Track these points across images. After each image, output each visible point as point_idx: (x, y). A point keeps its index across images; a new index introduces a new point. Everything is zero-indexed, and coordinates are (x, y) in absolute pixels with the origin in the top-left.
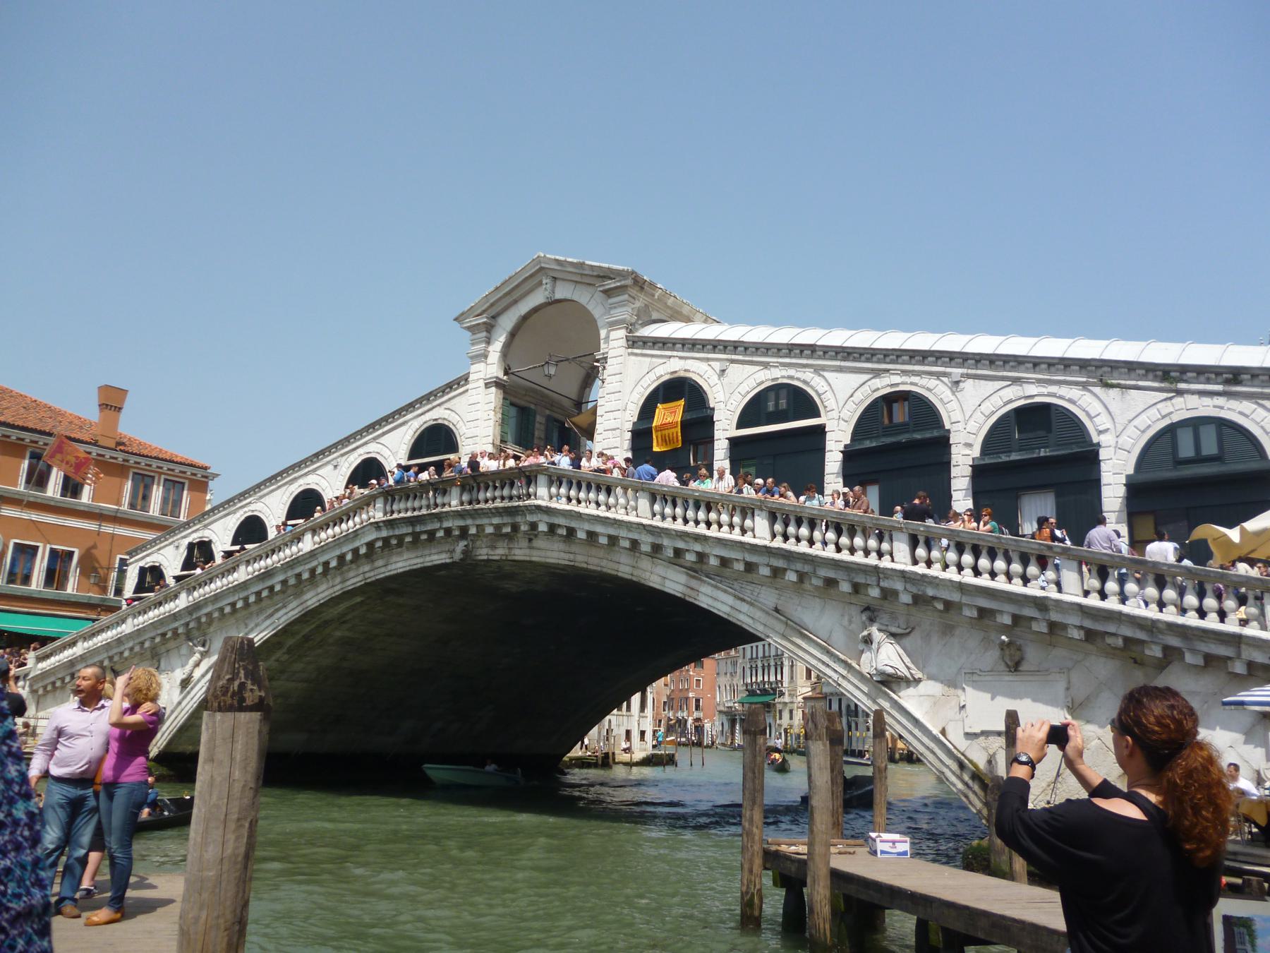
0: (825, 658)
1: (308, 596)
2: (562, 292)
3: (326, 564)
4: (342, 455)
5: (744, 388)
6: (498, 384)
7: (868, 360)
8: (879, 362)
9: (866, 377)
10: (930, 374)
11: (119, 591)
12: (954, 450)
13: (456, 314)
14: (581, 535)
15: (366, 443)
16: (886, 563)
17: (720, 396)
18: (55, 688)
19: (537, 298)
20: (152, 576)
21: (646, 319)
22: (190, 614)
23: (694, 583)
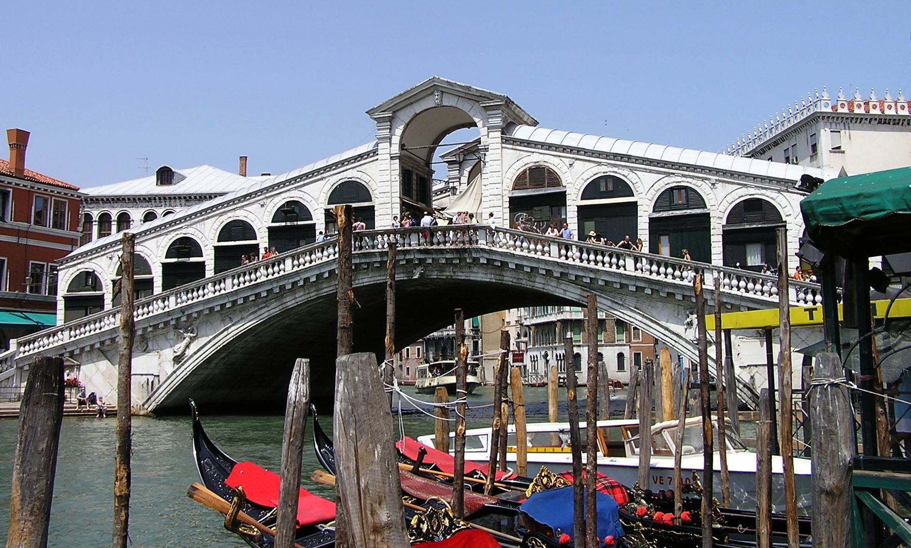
0: (667, 333)
1: (288, 299)
2: (448, 101)
3: (309, 278)
4: (267, 198)
5: (585, 176)
20: (89, 279)
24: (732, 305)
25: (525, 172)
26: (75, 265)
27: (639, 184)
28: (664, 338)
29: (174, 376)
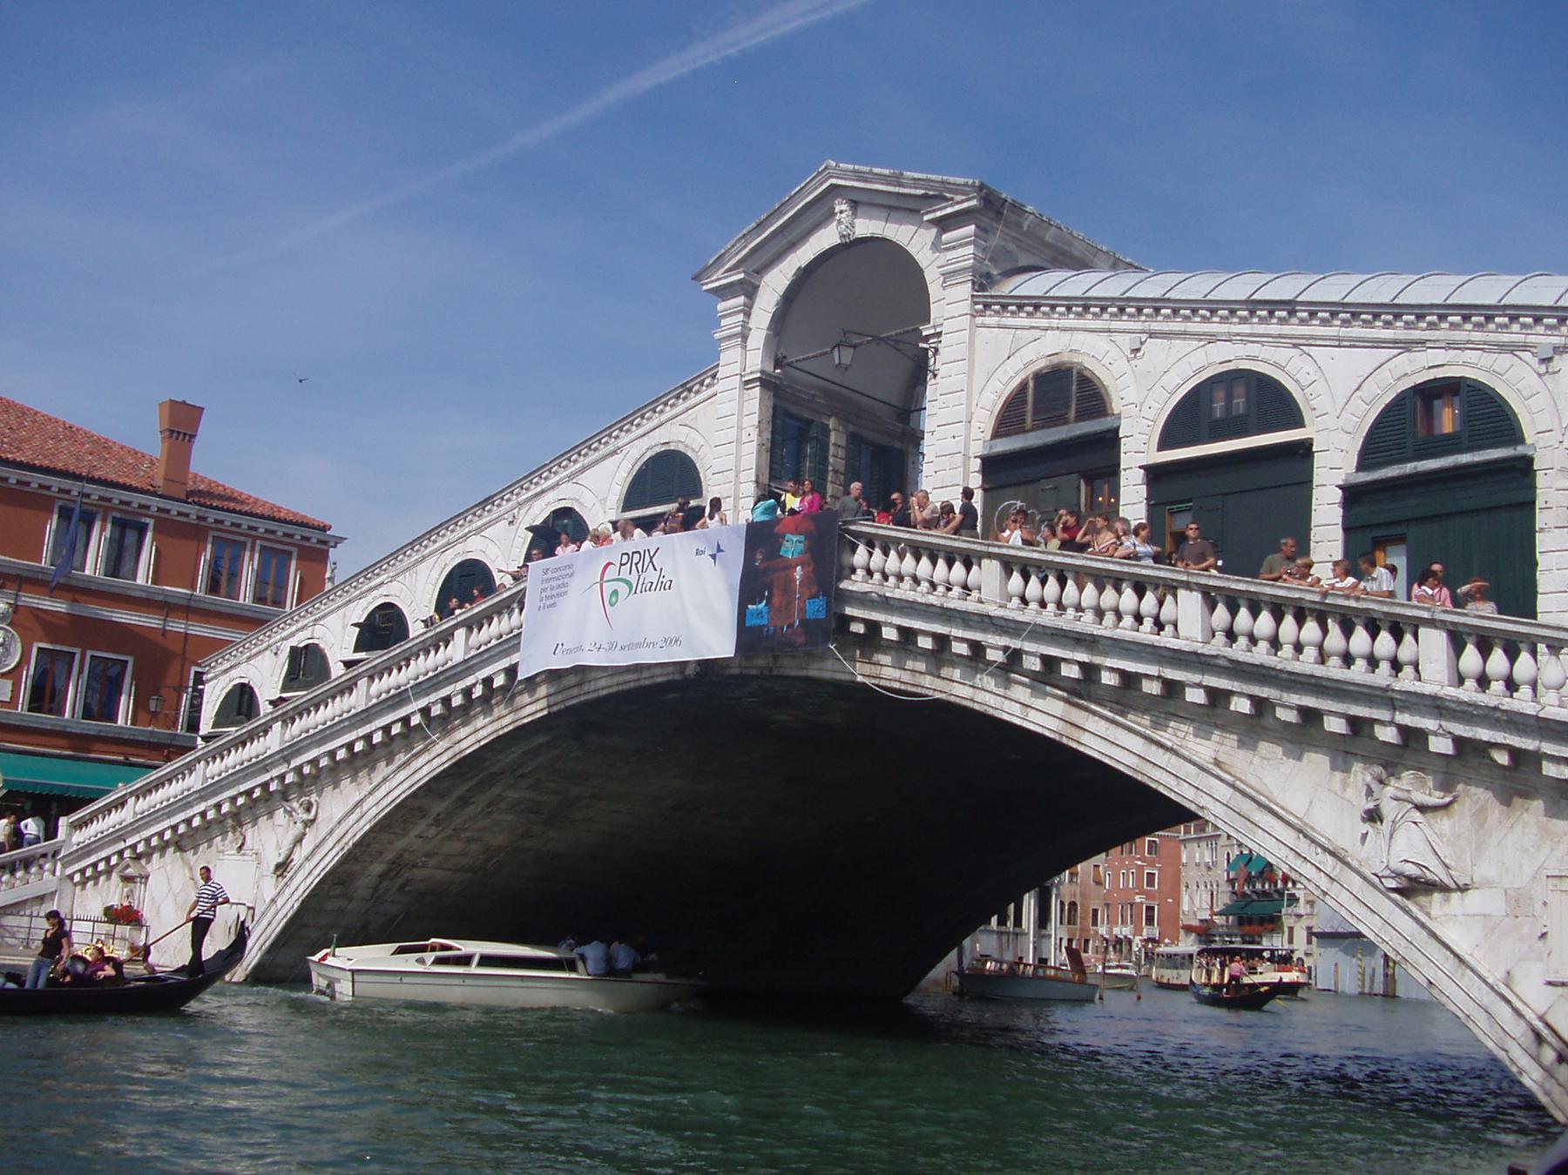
0: (1303, 846)
3: (488, 681)
4: (520, 504)
5: (1173, 379)
6: (765, 382)
7: (1388, 324)
8: (1408, 325)
9: (1385, 353)
10: (1503, 348)
11: (193, 726)
12: (1541, 480)
13: (696, 271)
14: (889, 634)
15: (558, 484)
16: (1406, 682)
17: (1131, 394)
18: (96, 877)
19: (826, 238)
20: (241, 702)
21: (1008, 266)
22: (287, 760)
23: (1077, 716)
24: (1514, 753)
25: (1023, 387)
26: (226, 671)
27: (1319, 387)
28: (1297, 864)
29: (273, 909)
